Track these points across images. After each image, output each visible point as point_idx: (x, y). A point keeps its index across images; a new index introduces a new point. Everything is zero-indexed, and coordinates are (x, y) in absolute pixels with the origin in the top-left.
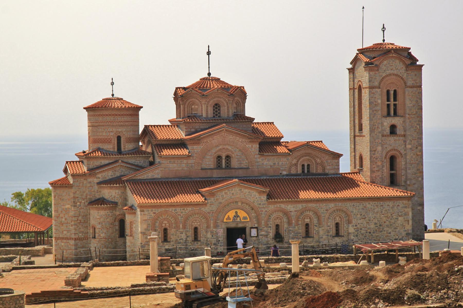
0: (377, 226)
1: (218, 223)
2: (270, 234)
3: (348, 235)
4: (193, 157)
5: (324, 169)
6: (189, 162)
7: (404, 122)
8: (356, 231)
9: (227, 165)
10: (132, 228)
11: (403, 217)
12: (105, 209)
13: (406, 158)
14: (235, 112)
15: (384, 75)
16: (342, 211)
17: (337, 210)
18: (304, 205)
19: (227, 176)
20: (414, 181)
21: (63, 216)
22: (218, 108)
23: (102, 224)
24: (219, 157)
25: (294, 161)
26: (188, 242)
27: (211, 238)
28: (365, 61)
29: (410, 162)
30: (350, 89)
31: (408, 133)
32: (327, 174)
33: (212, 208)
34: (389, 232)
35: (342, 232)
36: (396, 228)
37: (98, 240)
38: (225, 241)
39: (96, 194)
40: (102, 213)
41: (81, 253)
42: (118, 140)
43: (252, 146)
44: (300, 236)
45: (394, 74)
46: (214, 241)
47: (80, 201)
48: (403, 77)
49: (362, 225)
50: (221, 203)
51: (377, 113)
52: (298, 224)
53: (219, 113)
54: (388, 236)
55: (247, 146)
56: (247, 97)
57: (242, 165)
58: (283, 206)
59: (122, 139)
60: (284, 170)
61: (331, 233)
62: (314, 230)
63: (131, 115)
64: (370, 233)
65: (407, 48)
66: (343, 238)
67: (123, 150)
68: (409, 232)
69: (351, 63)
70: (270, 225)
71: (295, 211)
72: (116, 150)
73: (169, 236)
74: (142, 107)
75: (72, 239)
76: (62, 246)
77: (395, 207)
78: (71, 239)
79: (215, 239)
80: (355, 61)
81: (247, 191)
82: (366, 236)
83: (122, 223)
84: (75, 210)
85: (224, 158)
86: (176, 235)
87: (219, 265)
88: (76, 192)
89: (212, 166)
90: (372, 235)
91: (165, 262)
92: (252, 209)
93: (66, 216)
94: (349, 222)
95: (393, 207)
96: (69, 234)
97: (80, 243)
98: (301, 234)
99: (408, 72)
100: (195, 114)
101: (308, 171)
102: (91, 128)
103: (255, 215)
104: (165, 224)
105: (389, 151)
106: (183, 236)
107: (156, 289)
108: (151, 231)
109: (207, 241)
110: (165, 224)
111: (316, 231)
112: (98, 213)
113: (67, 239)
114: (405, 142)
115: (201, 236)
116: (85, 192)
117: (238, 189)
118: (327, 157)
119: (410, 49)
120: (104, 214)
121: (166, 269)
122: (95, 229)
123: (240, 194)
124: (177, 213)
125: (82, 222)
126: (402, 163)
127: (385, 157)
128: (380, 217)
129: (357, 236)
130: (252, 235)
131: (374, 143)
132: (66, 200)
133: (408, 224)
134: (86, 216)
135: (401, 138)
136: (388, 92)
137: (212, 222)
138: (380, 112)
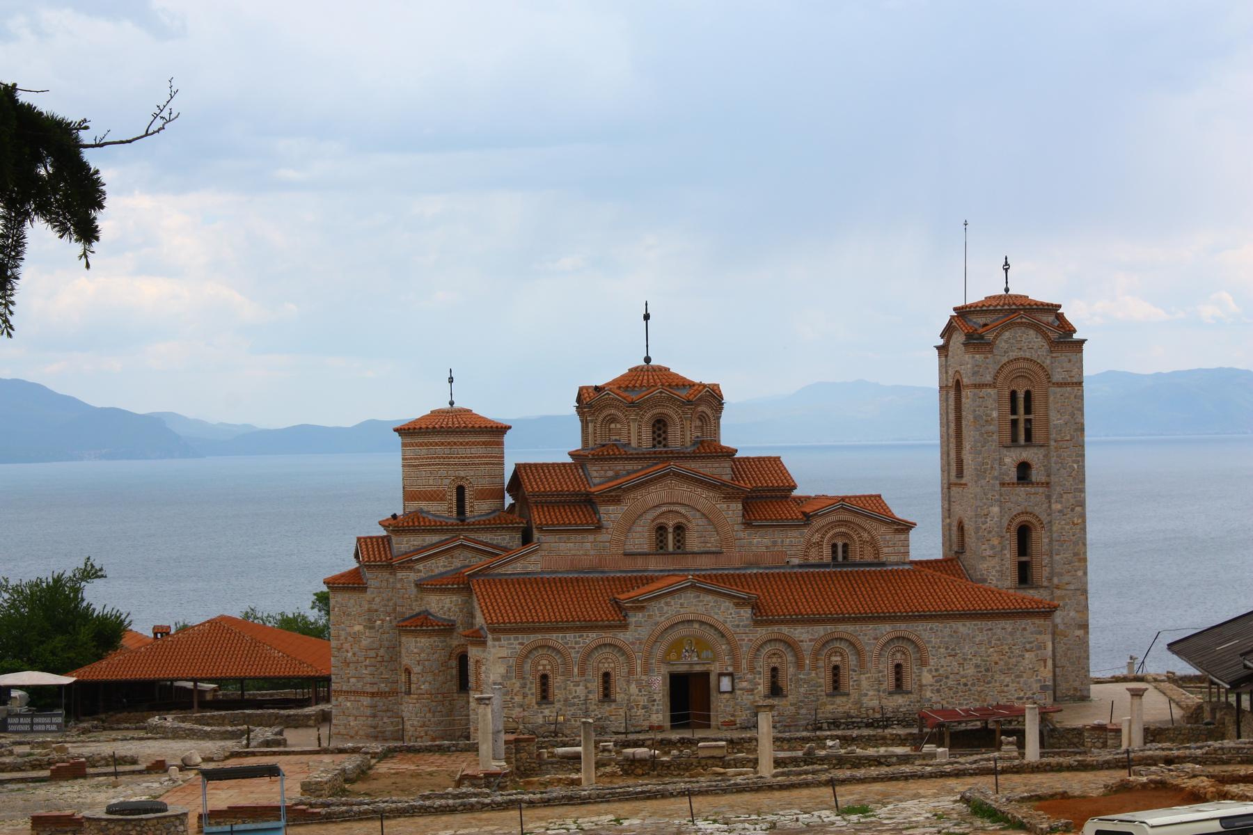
0: (980, 672)
1: (652, 664)
2: (759, 687)
3: (920, 690)
4: (607, 529)
5: (877, 553)
6: (598, 539)
7: (1046, 456)
8: (937, 682)
9: (678, 544)
11: (1035, 653)
12: (429, 633)
13: (1051, 531)
14: (698, 437)
15: (1005, 360)
16: (909, 640)
17: (898, 638)
18: (830, 628)
19: (677, 567)
20: (1067, 578)
21: (349, 648)
22: (663, 429)
23: (423, 665)
24: (661, 529)
25: (816, 538)
26: (591, 703)
27: (638, 695)
28: (966, 331)
29: (1058, 539)
30: (941, 387)
31: (1054, 479)
32: (883, 564)
33: (639, 634)
34: (1005, 684)
35: (908, 683)
36: (1018, 676)
37: (416, 696)
38: (667, 700)
39: (414, 604)
40: (424, 641)
42: (458, 494)
43: (728, 506)
44: (822, 691)
45: (1024, 359)
46: (643, 700)
47: (382, 617)
48: (1044, 365)
49: (949, 668)
50: (657, 624)
51: (990, 439)
52: (817, 668)
53: (665, 439)
54: (1004, 692)
55: (718, 506)
56: (725, 406)
57: (709, 545)
58: (785, 630)
59: (467, 493)
60: (795, 556)
61: (885, 686)
62: (850, 679)
63: (484, 443)
64: (965, 685)
65: (1052, 305)
66: (910, 695)
67: (468, 514)
68: (1047, 683)
69: (942, 336)
70: (758, 669)
71: (811, 640)
72: (455, 514)
73: (551, 690)
74: (510, 427)
75: (367, 693)
76: (348, 708)
77: (1018, 633)
78: (364, 693)
79: (646, 698)
80: (948, 332)
81: (709, 598)
82: (958, 692)
83: (463, 660)
84: (373, 635)
85: (671, 530)
86: (565, 689)
87: (634, 754)
88: (374, 598)
89: (646, 549)
90: (970, 690)
91: (525, 744)
92: (723, 636)
93: (356, 650)
94: (923, 662)
95: (1010, 632)
96: (360, 685)
97: (380, 702)
98: (824, 688)
99: (1054, 355)
100: (616, 440)
101: (845, 558)
102: (407, 469)
103: (728, 648)
104: (544, 666)
105: (1015, 516)
106: (580, 690)
107: (457, 805)
108: (514, 681)
109: (629, 700)
110: (544, 665)
111: (855, 681)
112: (416, 642)
113: (356, 693)
114: (1049, 497)
115: (618, 690)
116: (392, 599)
117: (692, 595)
118: (883, 529)
119: (1060, 306)
121: (527, 758)
122: (410, 673)
123: (695, 605)
124: (567, 643)
126: (1044, 540)
127: (1008, 529)
128: (987, 652)
129: (938, 691)
130: (722, 689)
131: (985, 501)
133: (1045, 667)
135: (1041, 490)
136: (1013, 395)
137: (639, 661)
138: (995, 437)
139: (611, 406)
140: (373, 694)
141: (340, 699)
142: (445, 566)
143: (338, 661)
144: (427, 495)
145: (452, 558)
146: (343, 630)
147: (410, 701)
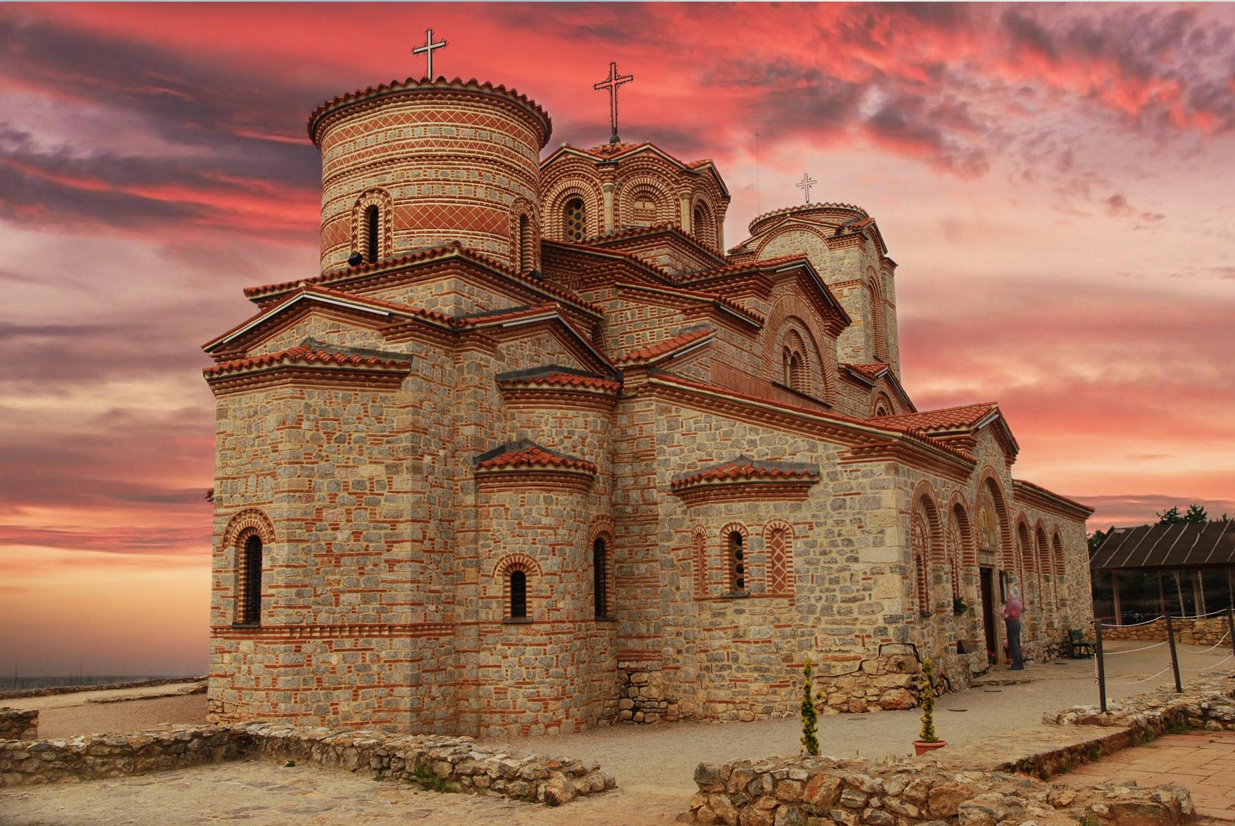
6: (753, 351)
10: (779, 558)
21: (343, 518)
23: (563, 553)
37: (547, 627)
41: (433, 699)
75: (391, 628)
76: (333, 671)
88: (422, 401)
96: (371, 609)
112: (548, 501)
113: (357, 629)
120: (568, 508)
125: (437, 547)
132: (362, 440)
134: (450, 521)
139: (647, 171)
140: (414, 627)
141: (307, 648)
142: (532, 360)
143: (307, 551)
144: (470, 218)
145: (538, 340)
146: (324, 475)
147: (529, 639)
